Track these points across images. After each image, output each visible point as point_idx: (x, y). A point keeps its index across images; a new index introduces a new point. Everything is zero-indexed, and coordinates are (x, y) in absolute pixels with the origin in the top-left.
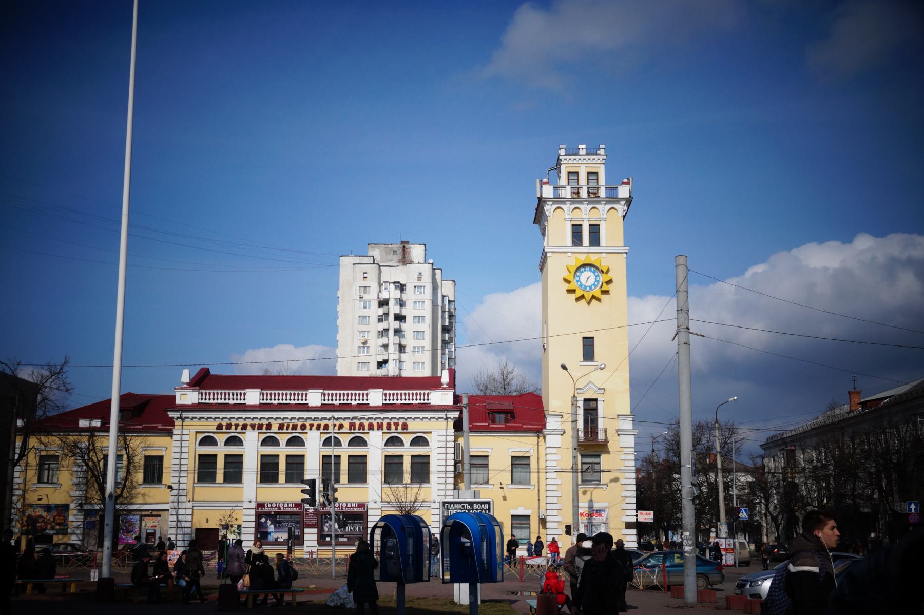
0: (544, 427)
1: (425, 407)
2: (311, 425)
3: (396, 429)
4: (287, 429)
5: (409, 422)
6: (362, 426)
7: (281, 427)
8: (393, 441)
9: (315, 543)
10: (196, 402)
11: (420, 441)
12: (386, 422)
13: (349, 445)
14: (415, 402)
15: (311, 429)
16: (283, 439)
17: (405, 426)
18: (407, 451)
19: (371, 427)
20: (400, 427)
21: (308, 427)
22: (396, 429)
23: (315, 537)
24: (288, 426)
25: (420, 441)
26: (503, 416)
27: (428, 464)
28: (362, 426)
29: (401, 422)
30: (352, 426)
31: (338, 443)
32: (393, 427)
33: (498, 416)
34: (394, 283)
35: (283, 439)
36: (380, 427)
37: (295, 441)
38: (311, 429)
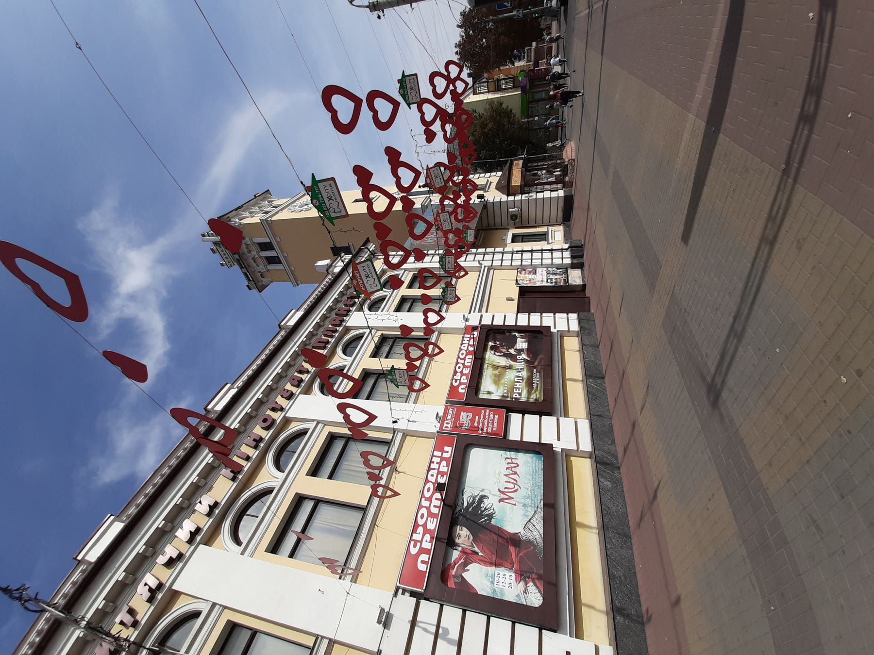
4: (248, 458)
9: (549, 422)
15: (282, 409)
23: (532, 420)
38: (282, 409)
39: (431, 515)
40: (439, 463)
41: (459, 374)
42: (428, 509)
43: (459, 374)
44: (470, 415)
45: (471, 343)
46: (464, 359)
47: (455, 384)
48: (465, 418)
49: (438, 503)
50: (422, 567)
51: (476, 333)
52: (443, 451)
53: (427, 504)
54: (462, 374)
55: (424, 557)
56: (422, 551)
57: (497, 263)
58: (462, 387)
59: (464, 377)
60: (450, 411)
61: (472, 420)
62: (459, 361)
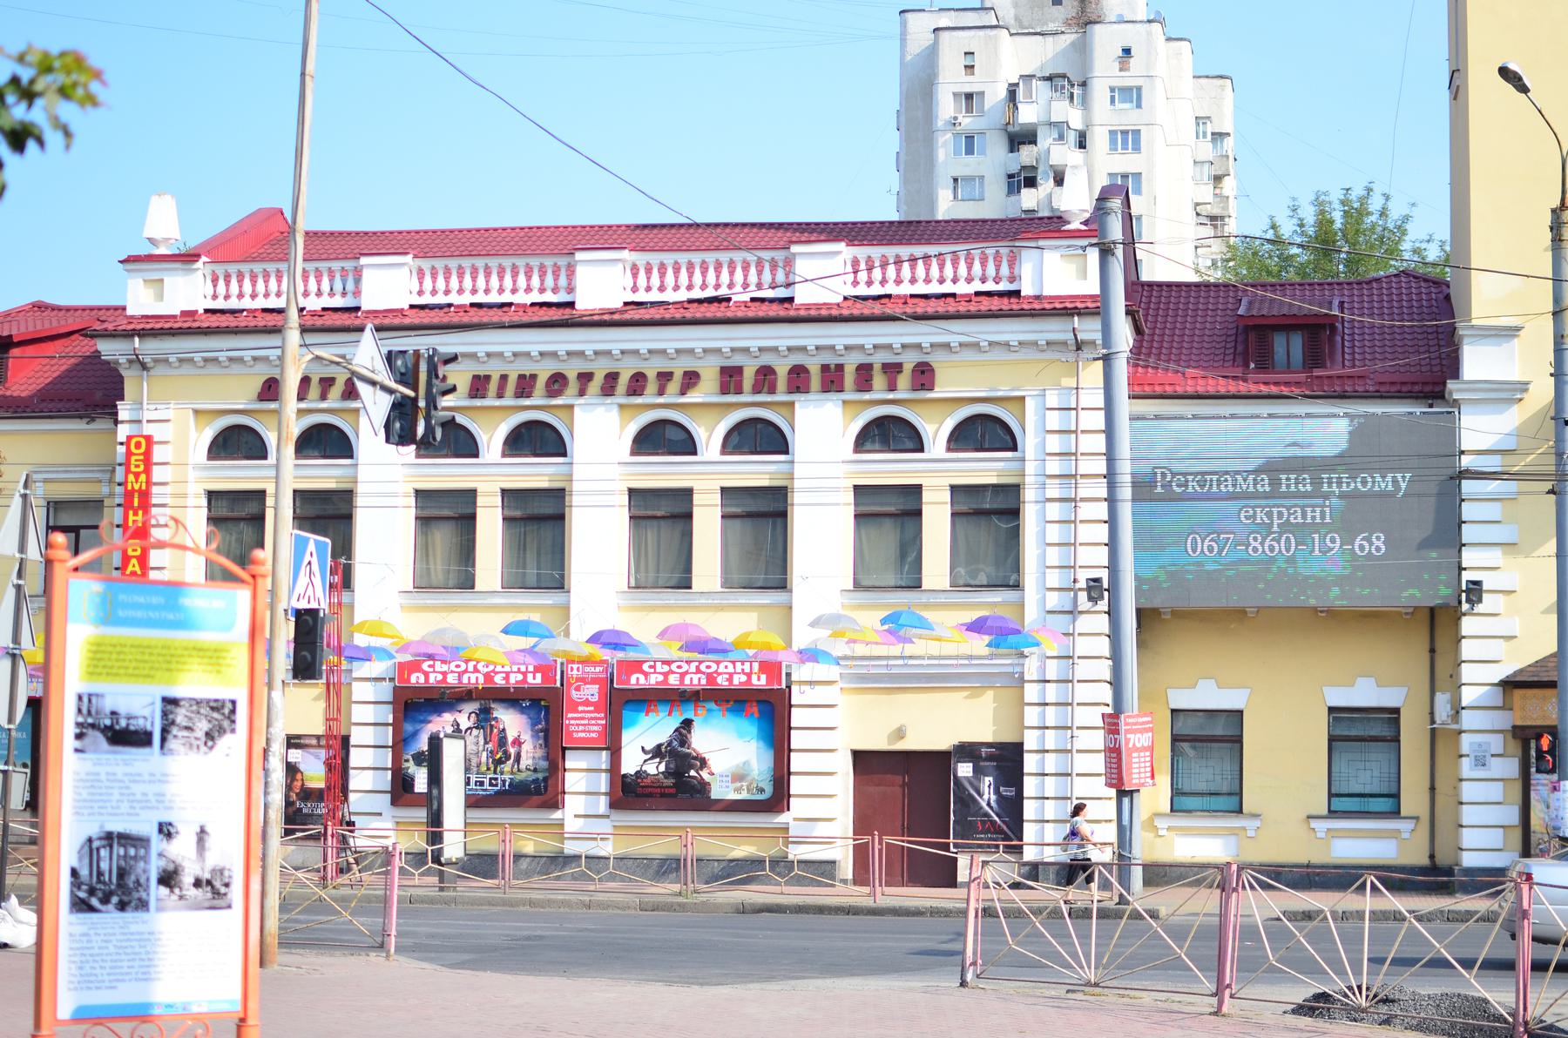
0: (1453, 367)
1: (1009, 304)
2: (585, 377)
3: (892, 387)
5: (935, 359)
6: (765, 378)
7: (479, 386)
8: (889, 434)
10: (200, 305)
11: (984, 431)
12: (851, 362)
13: (724, 451)
14: (962, 288)
16: (492, 437)
17: (924, 376)
18: (938, 472)
19: (799, 380)
20: (904, 380)
21: (573, 386)
22: (892, 387)
24: (504, 378)
25: (984, 431)
26: (1297, 341)
27: (1014, 513)
28: (765, 378)
29: (909, 360)
30: (730, 378)
31: (687, 445)
32: (879, 380)
33: (1279, 342)
34: (1050, 78)
35: (492, 437)
36: (832, 379)
37: (536, 439)
39: (461, 674)
40: (519, 671)
41: (666, 668)
42: (466, 671)
43: (666, 668)
44: (596, 699)
45: (736, 680)
46: (698, 671)
47: (645, 667)
48: (592, 692)
49: (473, 681)
50: (413, 679)
51: (760, 681)
52: (534, 673)
53: (471, 668)
54: (666, 675)
55: (422, 680)
56: (426, 674)
57: (1031, 692)
58: (642, 677)
59: (661, 678)
60: (598, 669)
61: (587, 703)
62: (693, 665)
